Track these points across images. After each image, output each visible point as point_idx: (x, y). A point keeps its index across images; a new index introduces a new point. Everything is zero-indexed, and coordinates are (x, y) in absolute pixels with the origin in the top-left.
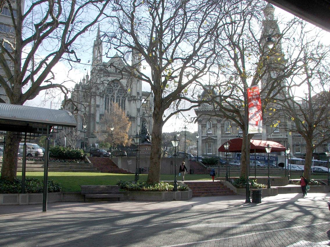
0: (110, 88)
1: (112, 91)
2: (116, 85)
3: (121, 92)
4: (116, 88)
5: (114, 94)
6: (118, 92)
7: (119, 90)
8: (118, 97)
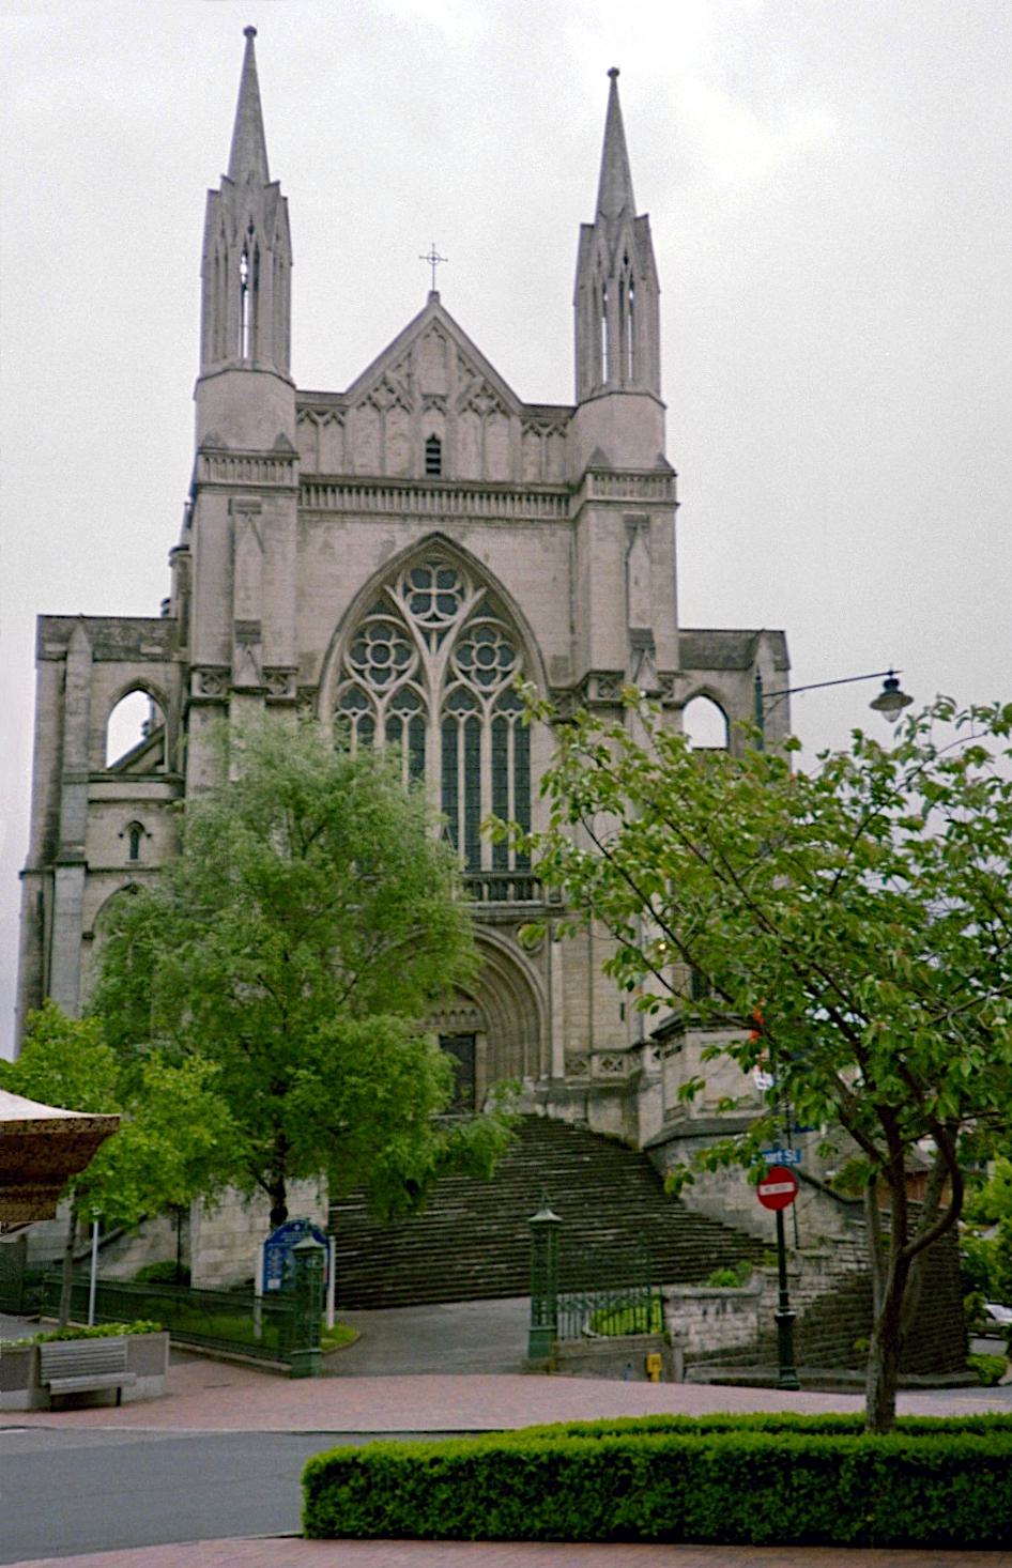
0: (382, 629)
1: (405, 653)
2: (434, 591)
3: (486, 654)
4: (435, 618)
5: (419, 677)
6: (462, 653)
7: (464, 635)
8: (462, 697)
